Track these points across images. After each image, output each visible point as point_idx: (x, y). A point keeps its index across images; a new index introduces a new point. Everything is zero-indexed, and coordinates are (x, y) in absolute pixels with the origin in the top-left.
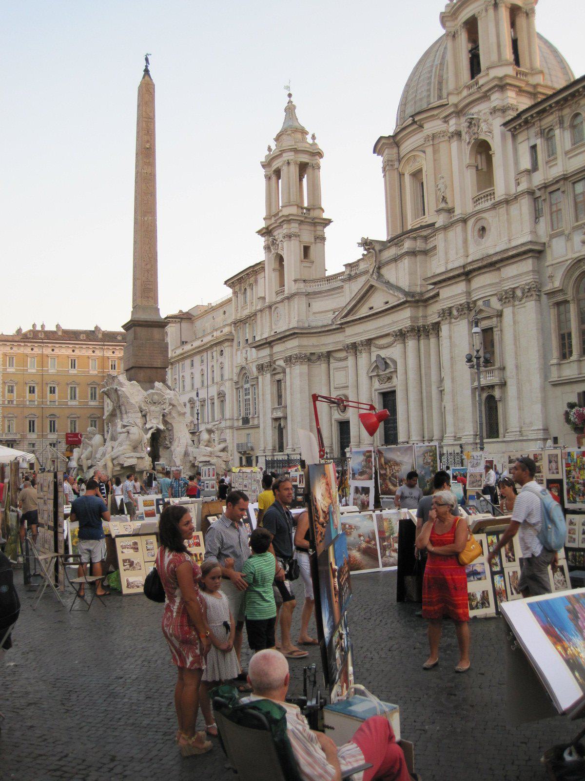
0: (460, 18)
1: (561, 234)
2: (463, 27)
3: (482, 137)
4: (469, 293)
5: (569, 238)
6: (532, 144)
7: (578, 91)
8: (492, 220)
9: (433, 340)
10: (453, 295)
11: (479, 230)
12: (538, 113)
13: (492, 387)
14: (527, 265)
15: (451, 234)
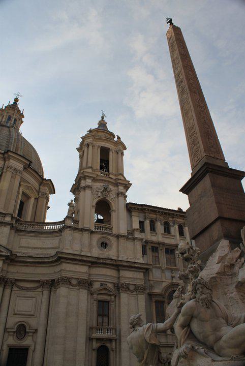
0: (98, 143)
1: (160, 268)
2: (101, 148)
3: (109, 199)
4: (90, 275)
5: (163, 271)
6: (142, 220)
7: (174, 214)
8: (113, 240)
9: (8, 291)
10: (81, 271)
11: (102, 244)
12: (151, 210)
13: (110, 340)
14: (140, 275)
15: (77, 235)
